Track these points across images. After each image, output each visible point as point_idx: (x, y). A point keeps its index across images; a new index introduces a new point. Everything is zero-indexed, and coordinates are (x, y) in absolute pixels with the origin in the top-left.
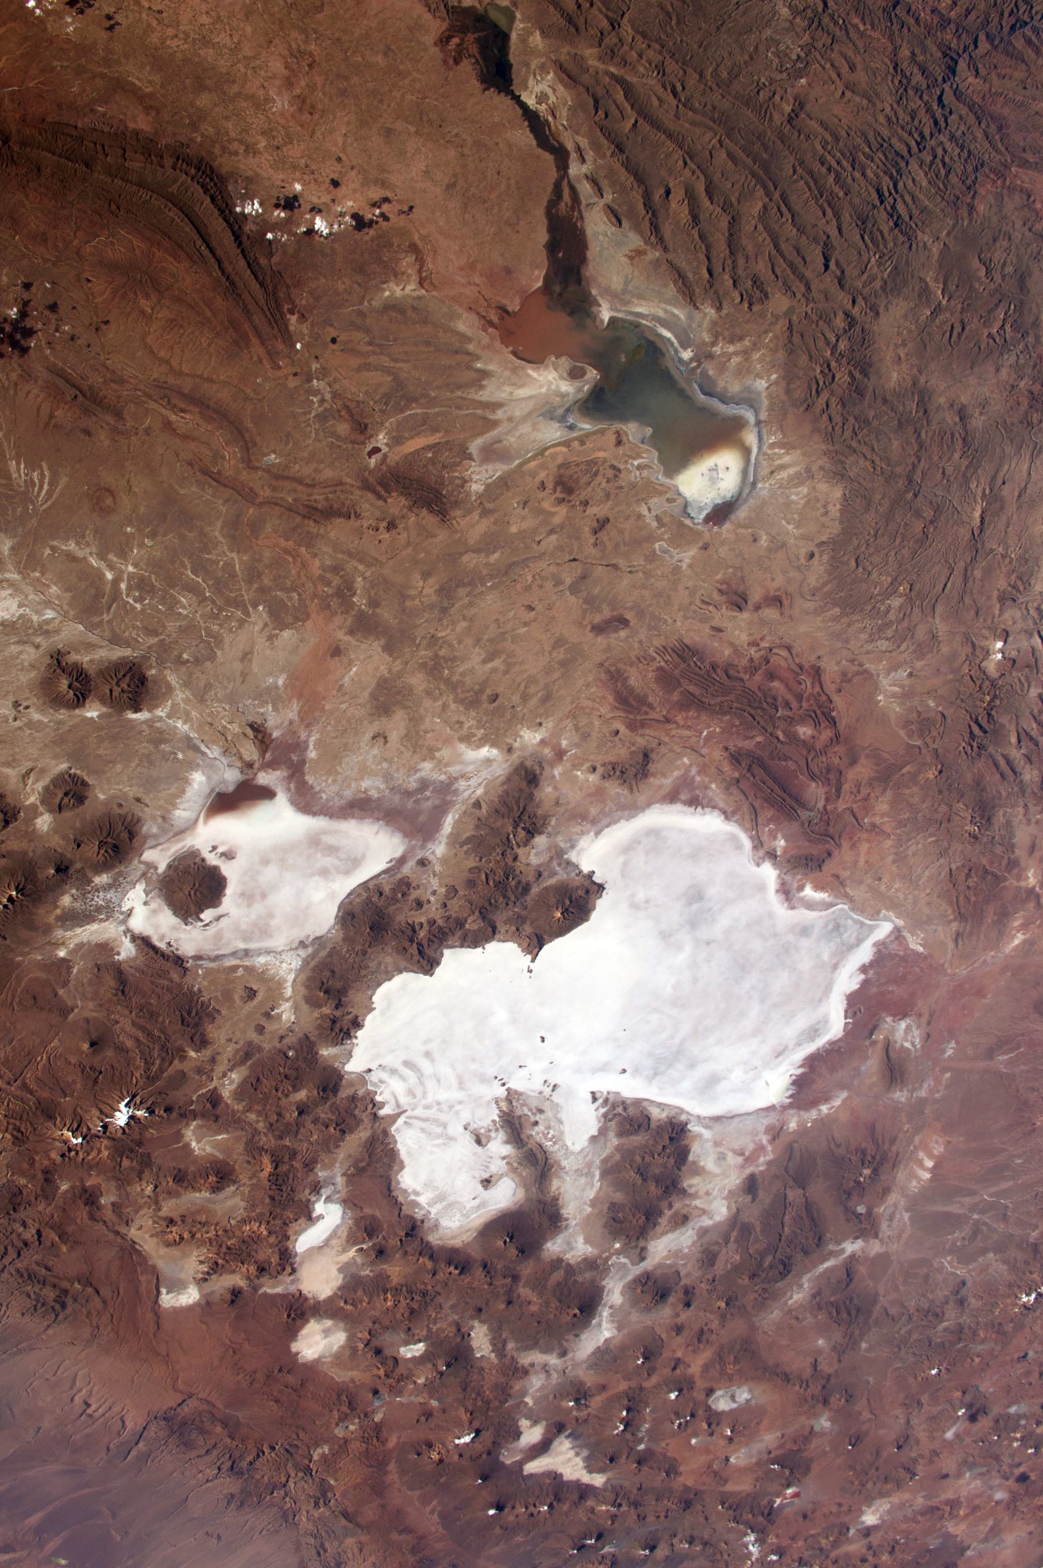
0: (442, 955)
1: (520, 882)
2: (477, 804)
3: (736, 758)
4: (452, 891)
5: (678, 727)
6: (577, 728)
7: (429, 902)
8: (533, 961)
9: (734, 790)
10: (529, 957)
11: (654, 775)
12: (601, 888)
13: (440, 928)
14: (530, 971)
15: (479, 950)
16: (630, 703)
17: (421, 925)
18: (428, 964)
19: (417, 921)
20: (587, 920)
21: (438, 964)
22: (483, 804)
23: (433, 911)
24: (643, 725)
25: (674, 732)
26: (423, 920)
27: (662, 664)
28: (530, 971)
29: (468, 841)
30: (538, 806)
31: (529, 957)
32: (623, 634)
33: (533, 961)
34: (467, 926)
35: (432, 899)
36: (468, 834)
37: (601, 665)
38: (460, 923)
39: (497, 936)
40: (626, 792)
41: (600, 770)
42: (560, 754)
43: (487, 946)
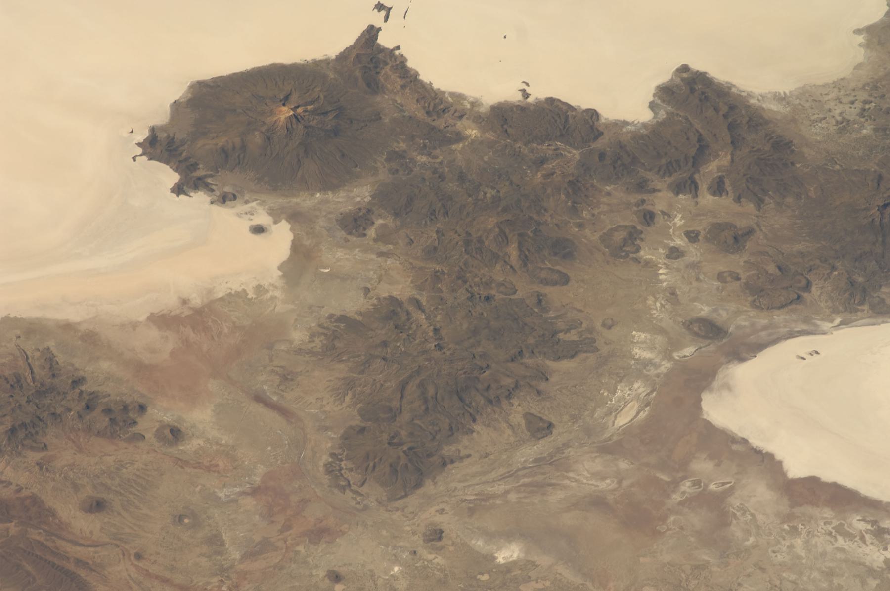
0: (652, 106)
7: (692, 236)
15: (539, 93)
17: (718, 188)
18: (692, 94)
19: (726, 202)
22: (517, 418)
23: (678, 215)
26: (707, 199)
30: (349, 384)
35: (679, 242)
36: (566, 365)
42: (271, 494)
43: (515, 97)
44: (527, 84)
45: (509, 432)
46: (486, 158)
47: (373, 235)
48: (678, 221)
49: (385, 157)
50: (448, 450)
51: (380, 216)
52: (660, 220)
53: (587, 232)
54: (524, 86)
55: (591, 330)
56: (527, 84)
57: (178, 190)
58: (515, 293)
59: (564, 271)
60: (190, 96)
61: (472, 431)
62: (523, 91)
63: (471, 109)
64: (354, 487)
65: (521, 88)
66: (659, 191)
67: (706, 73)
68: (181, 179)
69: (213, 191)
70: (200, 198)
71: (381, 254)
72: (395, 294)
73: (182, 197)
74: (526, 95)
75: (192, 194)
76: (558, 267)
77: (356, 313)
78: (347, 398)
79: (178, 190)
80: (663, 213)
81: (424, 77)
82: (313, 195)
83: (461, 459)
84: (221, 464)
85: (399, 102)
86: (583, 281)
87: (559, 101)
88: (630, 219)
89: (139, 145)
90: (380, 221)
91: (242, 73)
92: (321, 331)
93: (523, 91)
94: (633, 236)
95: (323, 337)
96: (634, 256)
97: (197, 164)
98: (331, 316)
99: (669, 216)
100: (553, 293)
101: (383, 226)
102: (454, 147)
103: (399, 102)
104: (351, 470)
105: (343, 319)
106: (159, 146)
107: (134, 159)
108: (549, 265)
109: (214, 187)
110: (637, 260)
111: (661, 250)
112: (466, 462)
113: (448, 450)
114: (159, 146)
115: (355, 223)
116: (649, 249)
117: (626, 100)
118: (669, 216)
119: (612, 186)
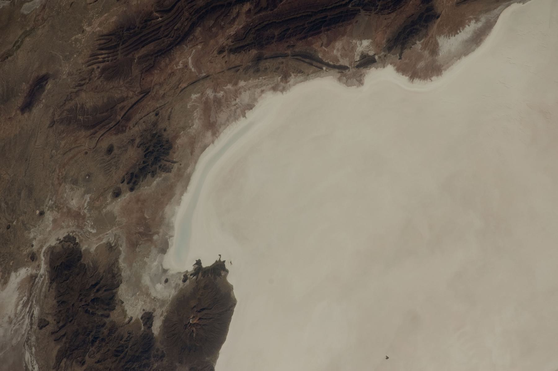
2: (43, 324)
3: (239, 45)
5: (161, 84)
6: (75, 182)
9: (264, 64)
11: (176, 137)
16: (103, 120)
22: (50, 319)
24: (127, 118)
25: (161, 92)
27: (101, 65)
32: (49, 86)
37: (53, 123)
40: (164, 175)
41: (124, 186)
45: (47, 312)
50: (54, 285)
51: (144, 331)
57: (199, 263)
61: (55, 298)
64: (63, 242)
68: (202, 267)
69: (191, 275)
72: (115, 311)
73: (195, 262)
78: (91, 264)
79: (199, 263)
82: (167, 312)
83: (50, 287)
84: (97, 203)
89: (224, 261)
90: (143, 329)
91: (229, 324)
92: (118, 274)
95: (116, 272)
97: (204, 277)
101: (141, 328)
104: (69, 246)
106: (219, 268)
107: (220, 255)
109: (192, 277)
112: (48, 288)
113: (54, 285)
114: (219, 268)
115: (148, 318)
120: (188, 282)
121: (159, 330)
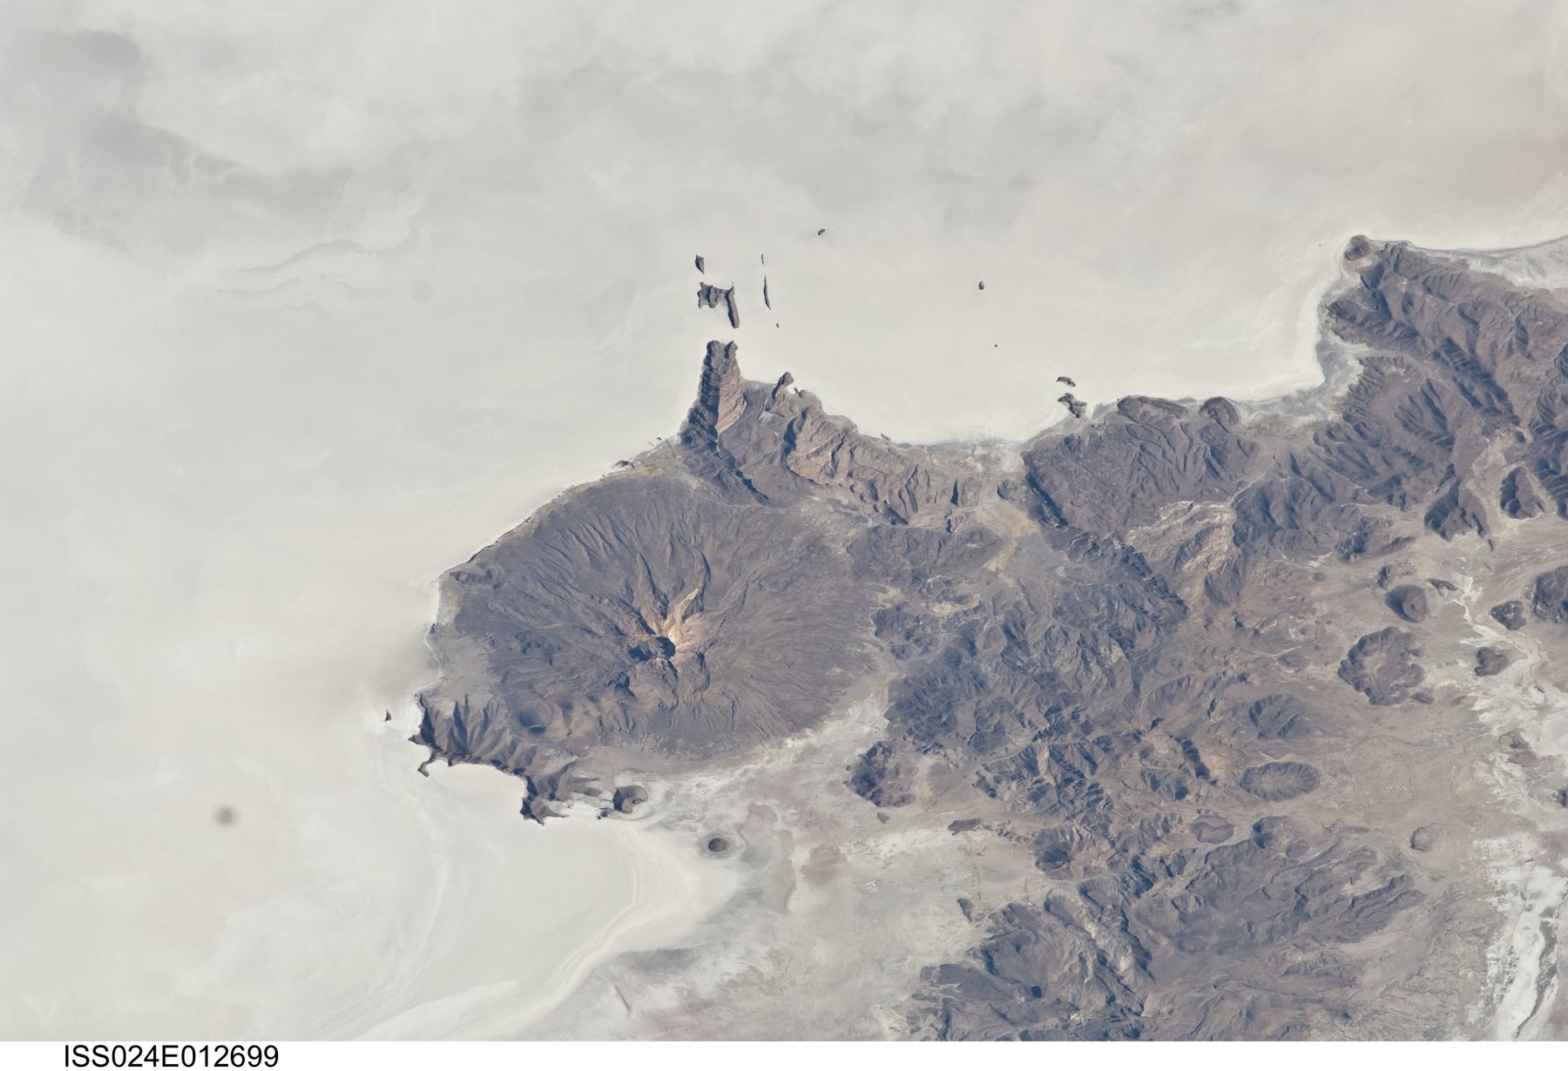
0: (1327, 357)
1: (980, 743)
4: (1381, 672)
8: (719, 360)
10: (755, 368)
12: (448, 738)
13: (1392, 491)
14: (708, 295)
15: (1099, 395)
20: (457, 578)
21: (1339, 311)
28: (708, 295)
29: (1368, 913)
31: (755, 368)
33: (719, 360)
34: (1223, 514)
36: (1378, 943)
38: (1263, 520)
39: (1012, 465)
44: (1069, 382)
46: (1060, 572)
47: (928, 793)
48: (1469, 589)
49: (874, 629)
52: (1437, 601)
53: (1311, 669)
54: (1064, 389)
55: (1396, 862)
56: (1069, 382)
58: (1230, 834)
59: (1301, 760)
60: (455, 609)
62: (1067, 398)
63: (986, 474)
65: (1062, 395)
66: (1409, 539)
67: (1405, 244)
68: (531, 788)
70: (579, 813)
71: (956, 827)
72: (1017, 898)
73: (548, 820)
74: (1075, 408)
75: (564, 811)
76: (1285, 759)
77: (968, 953)
80: (1437, 584)
81: (868, 425)
82: (780, 745)
85: (845, 502)
86: (1344, 770)
87: (1143, 400)
88: (1378, 618)
93: (1067, 398)
94: (1404, 653)
96: (1417, 690)
98: (927, 971)
99: (1450, 587)
100: (1302, 815)
101: (936, 771)
102: (992, 566)
103: (845, 502)
105: (948, 972)
108: (1270, 760)
109: (593, 785)
110: (1422, 698)
111: (1462, 664)
116: (1440, 666)
117: (1271, 358)
118: (1450, 587)
119: (1321, 558)
120: (622, 781)
121: (854, 712)
